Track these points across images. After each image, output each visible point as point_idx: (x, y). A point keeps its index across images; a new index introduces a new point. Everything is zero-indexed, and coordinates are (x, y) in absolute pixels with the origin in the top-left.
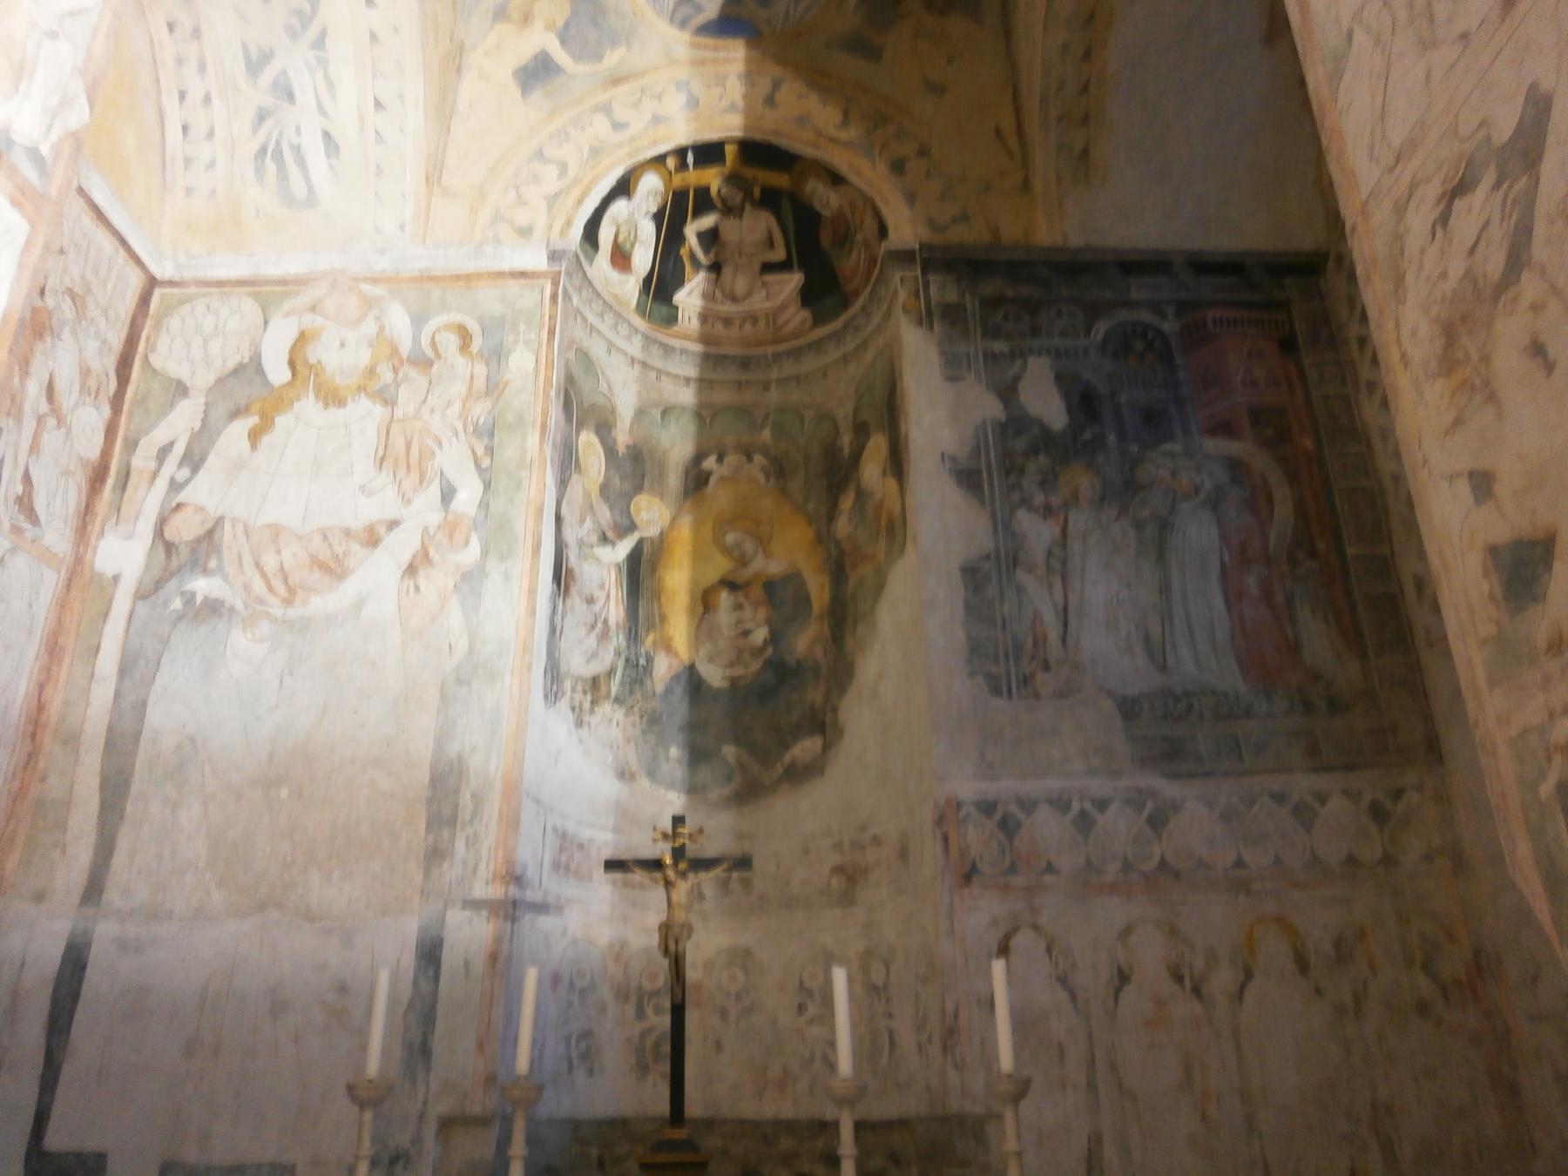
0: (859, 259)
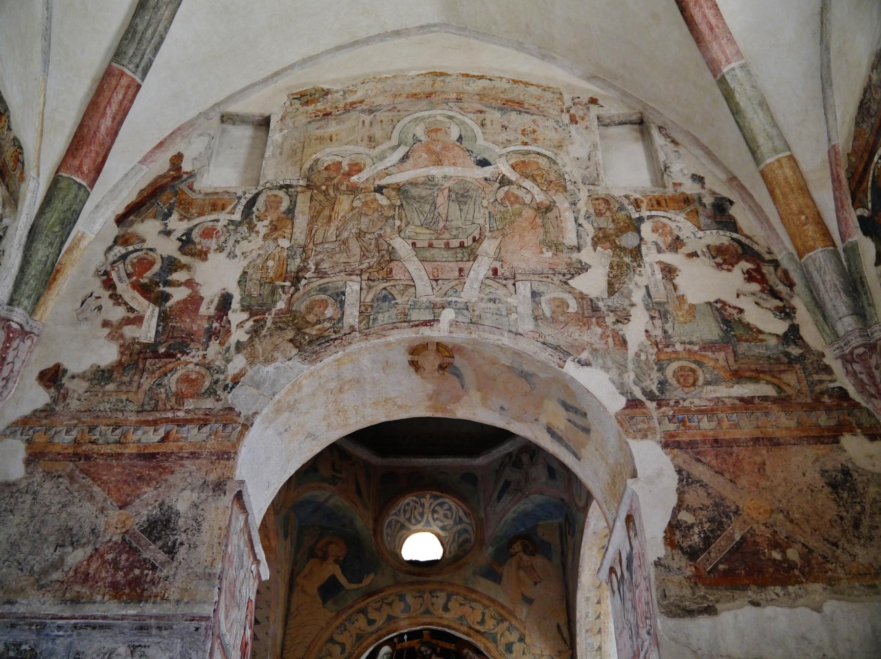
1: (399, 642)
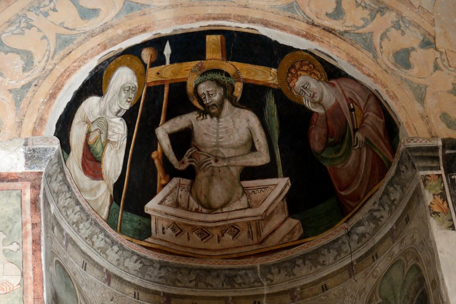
0: (360, 160)
1: (153, 65)
